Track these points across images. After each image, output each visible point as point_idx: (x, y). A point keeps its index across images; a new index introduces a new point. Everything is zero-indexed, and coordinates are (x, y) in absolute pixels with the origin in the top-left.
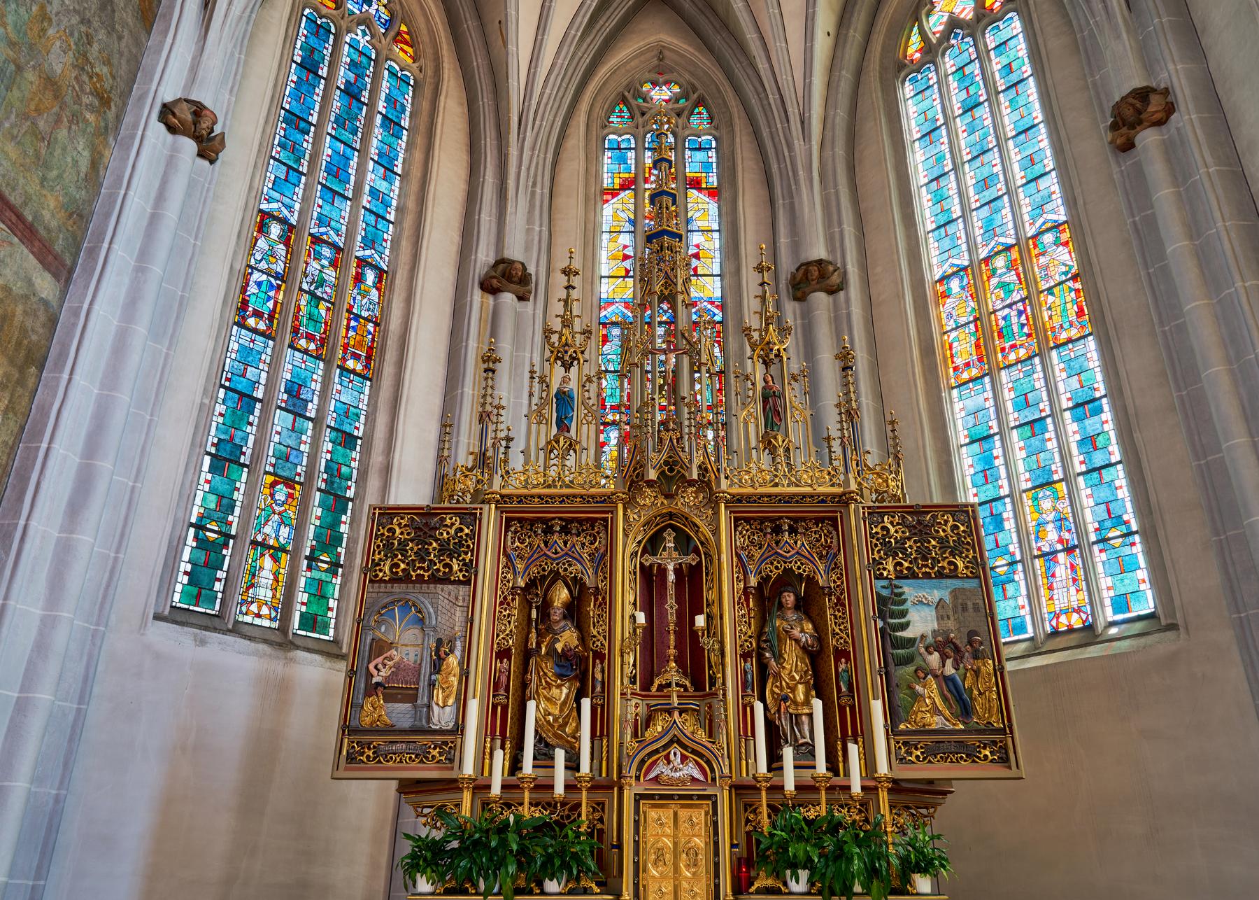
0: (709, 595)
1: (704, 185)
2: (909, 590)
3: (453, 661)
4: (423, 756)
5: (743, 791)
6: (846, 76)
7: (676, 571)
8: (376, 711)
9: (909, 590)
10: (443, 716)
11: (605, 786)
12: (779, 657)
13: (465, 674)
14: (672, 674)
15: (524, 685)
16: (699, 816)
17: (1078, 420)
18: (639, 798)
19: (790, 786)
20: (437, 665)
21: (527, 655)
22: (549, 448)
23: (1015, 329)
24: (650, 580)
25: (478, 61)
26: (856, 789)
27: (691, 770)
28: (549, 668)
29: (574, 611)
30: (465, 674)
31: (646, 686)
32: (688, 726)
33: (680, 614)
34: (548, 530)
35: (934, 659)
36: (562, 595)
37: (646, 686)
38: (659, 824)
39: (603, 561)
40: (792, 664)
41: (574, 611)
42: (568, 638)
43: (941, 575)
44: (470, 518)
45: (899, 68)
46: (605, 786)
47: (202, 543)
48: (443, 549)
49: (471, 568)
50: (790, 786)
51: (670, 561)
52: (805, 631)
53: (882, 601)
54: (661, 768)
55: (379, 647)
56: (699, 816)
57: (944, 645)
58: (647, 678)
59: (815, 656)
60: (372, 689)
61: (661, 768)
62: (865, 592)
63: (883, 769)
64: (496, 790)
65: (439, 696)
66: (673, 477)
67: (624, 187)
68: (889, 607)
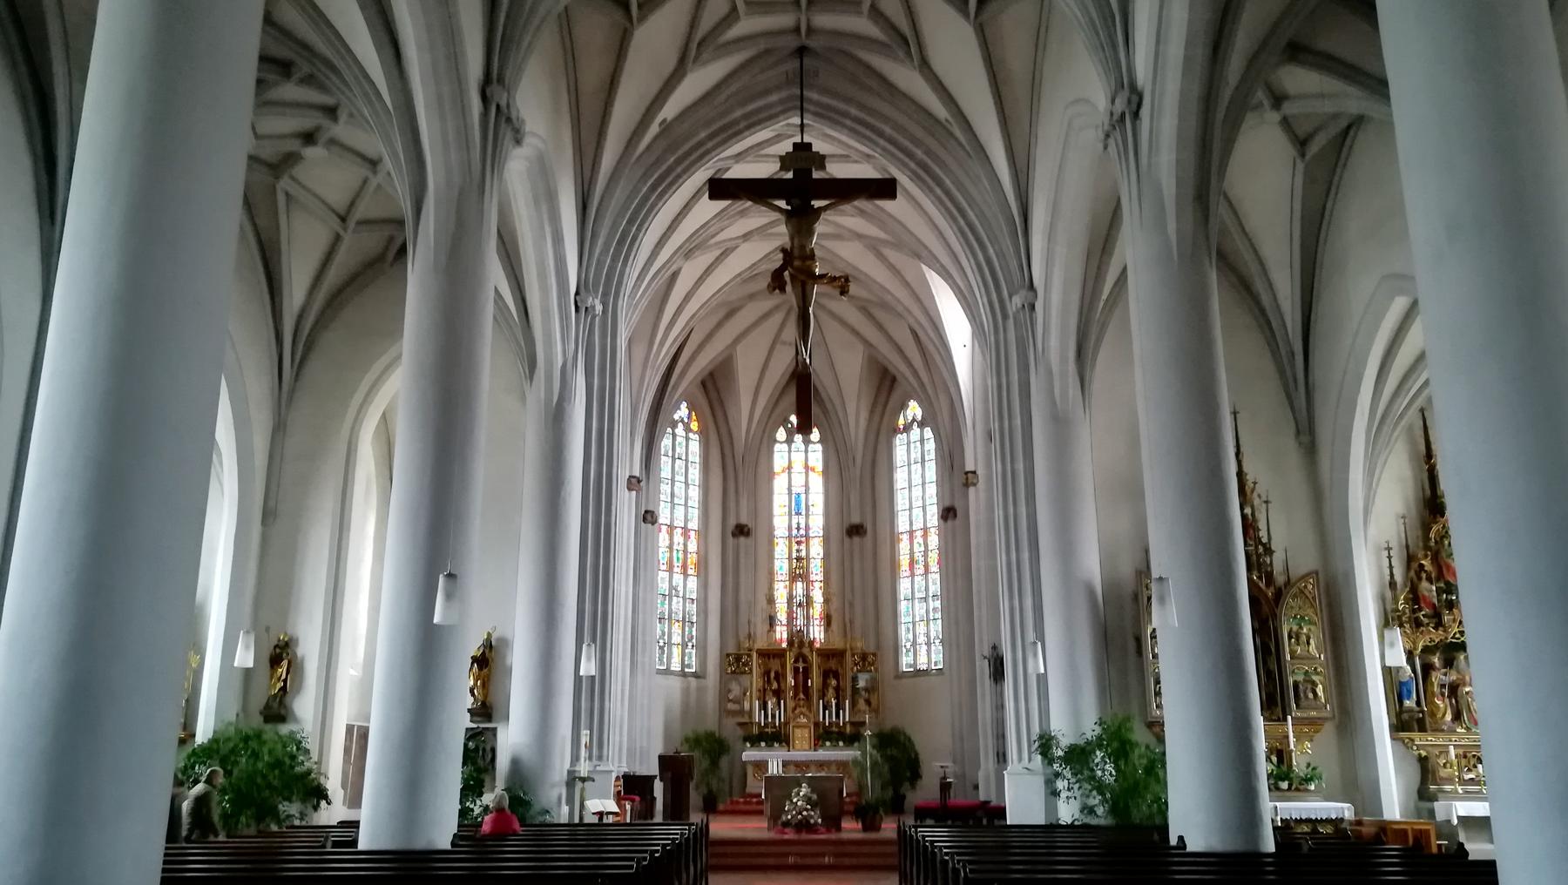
0: (811, 676)
1: (816, 470)
2: (860, 675)
3: (748, 694)
4: (743, 716)
5: (817, 724)
6: (872, 437)
7: (803, 668)
8: (731, 706)
9: (860, 675)
10: (747, 706)
11: (787, 723)
12: (828, 691)
13: (751, 697)
14: (802, 696)
15: (764, 698)
16: (807, 731)
17: (933, 601)
18: (793, 727)
19: (827, 724)
20: (745, 694)
21: (765, 690)
22: (769, 631)
23: (920, 562)
24: (796, 670)
25: (723, 430)
26: (841, 724)
27: (805, 720)
28: (771, 694)
29: (777, 677)
30: (751, 697)
31: (795, 699)
32: (804, 710)
33: (803, 680)
34: (769, 658)
35: (863, 693)
36: (772, 675)
37: (795, 699)
38: (798, 732)
39: (784, 666)
40: (831, 692)
41: (777, 677)
42: (775, 686)
43: (868, 671)
44: (749, 656)
45: (896, 431)
46: (787, 723)
47: (660, 647)
48: (743, 663)
49: (751, 670)
50: (827, 724)
51: (801, 665)
52: (834, 682)
53: (853, 678)
54: (799, 720)
55: (729, 691)
56: (807, 731)
57: (866, 690)
58: (796, 694)
59: (837, 689)
60: (730, 701)
61: (799, 720)
62: (849, 675)
63: (847, 719)
64: (763, 724)
65: (745, 703)
66: (801, 644)
67: (783, 471)
68: (855, 679)
